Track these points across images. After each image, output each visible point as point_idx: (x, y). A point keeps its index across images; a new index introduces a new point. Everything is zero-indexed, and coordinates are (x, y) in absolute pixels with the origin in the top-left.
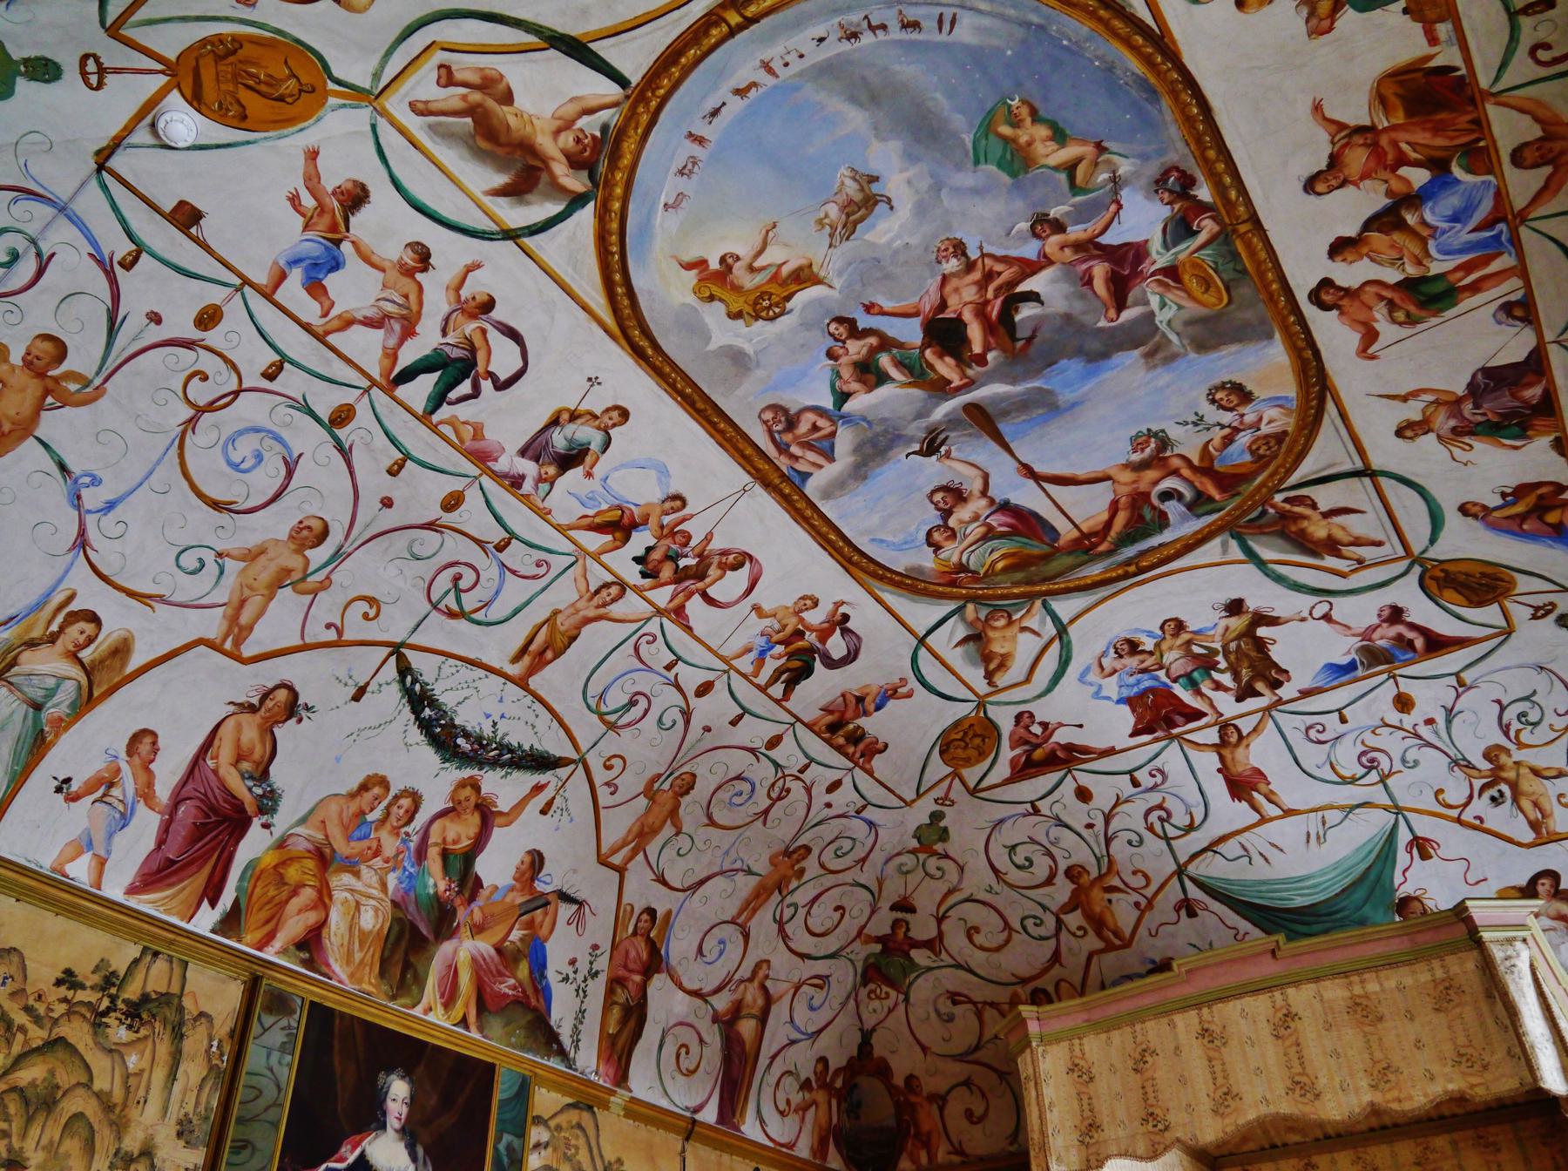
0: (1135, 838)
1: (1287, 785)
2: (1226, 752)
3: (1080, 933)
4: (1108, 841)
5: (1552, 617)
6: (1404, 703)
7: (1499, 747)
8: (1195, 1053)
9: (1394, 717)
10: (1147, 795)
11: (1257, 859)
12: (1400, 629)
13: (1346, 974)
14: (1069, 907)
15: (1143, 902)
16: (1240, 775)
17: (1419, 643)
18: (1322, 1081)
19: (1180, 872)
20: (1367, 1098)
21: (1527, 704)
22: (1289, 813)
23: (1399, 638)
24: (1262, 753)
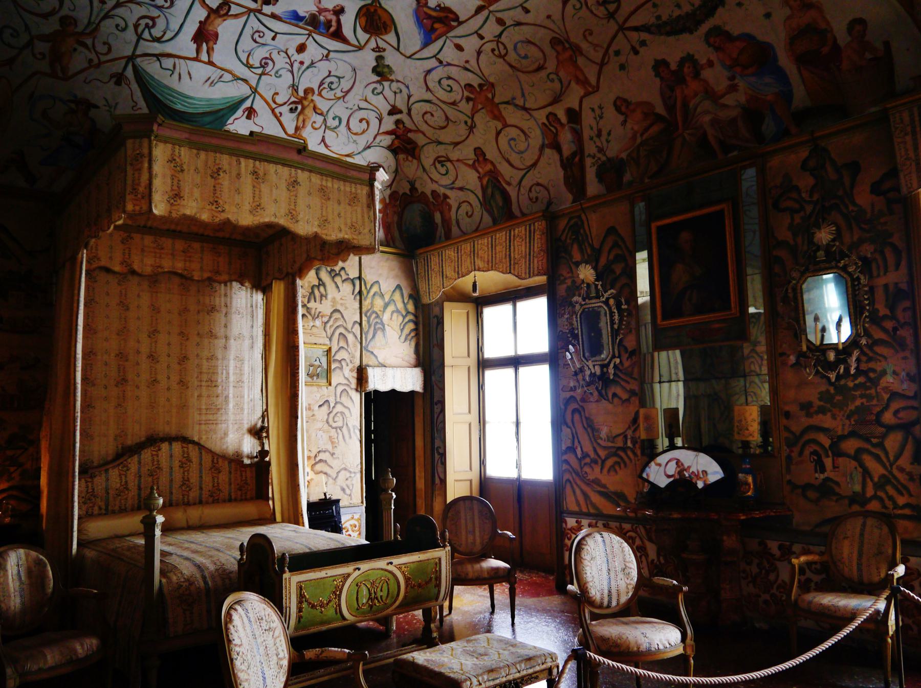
0: (123, 24)
1: (223, 52)
2: (212, 16)
3: (38, 56)
4: (106, 16)
5: (378, 54)
6: (301, 48)
7: (312, 90)
8: (247, 181)
9: (292, 51)
10: (152, 9)
11: (176, 76)
12: (334, 18)
13: (322, 174)
14: (44, 38)
15: (96, 61)
16: (207, 31)
17: (332, 29)
18: (301, 216)
19: (131, 58)
20: (315, 230)
21: (337, 80)
22: (210, 63)
23: (330, 22)
24: (227, 29)
